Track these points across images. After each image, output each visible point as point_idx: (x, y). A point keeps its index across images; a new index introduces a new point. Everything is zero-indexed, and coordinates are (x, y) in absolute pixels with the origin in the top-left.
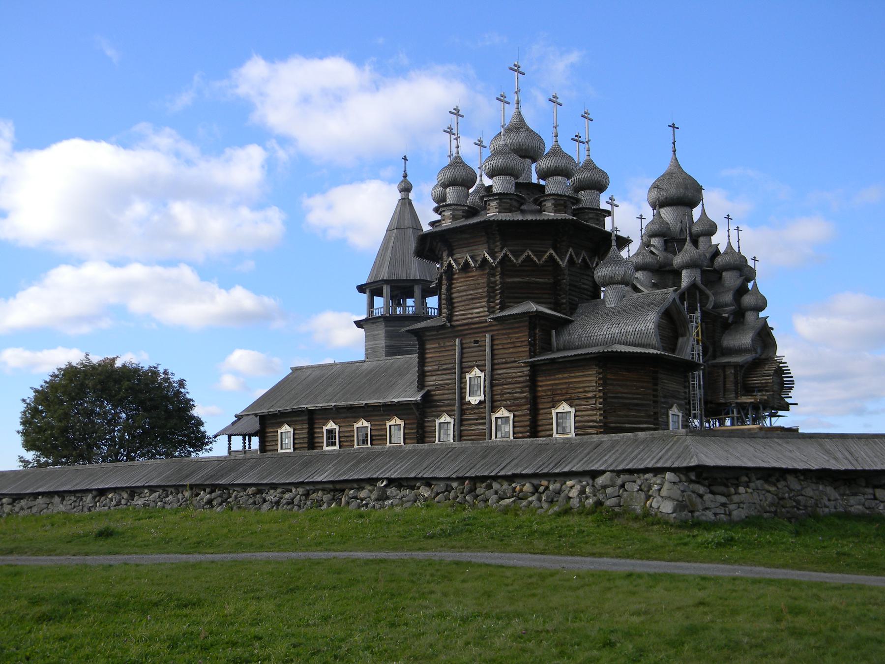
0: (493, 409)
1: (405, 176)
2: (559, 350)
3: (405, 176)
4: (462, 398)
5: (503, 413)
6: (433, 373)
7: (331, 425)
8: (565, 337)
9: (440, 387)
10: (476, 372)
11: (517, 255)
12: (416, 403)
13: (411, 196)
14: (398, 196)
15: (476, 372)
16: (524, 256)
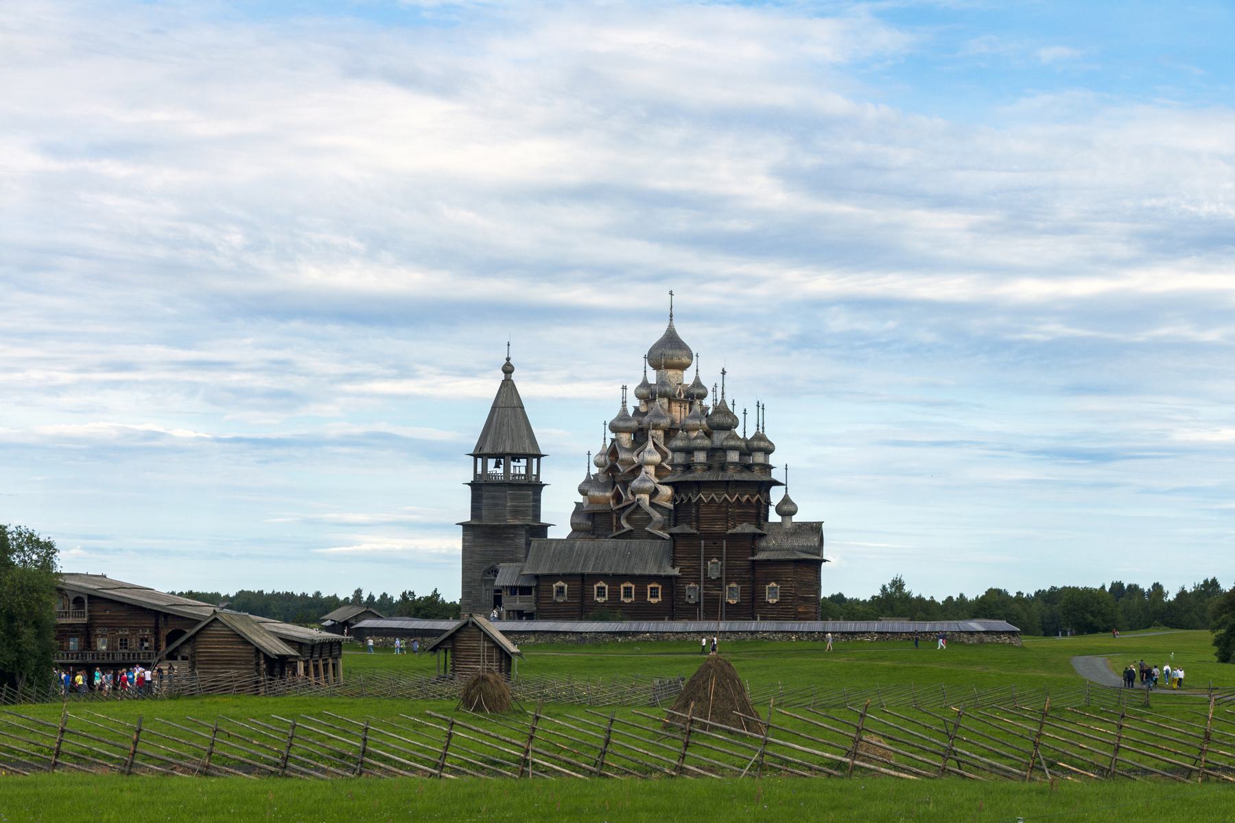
0: (728, 582)
1: (508, 359)
2: (763, 550)
3: (508, 359)
4: (706, 574)
5: (733, 585)
6: (683, 558)
7: (601, 584)
8: (763, 544)
9: (688, 567)
10: (715, 560)
11: (742, 496)
12: (676, 577)
13: (514, 376)
14: (502, 376)
15: (715, 560)
16: (746, 497)
